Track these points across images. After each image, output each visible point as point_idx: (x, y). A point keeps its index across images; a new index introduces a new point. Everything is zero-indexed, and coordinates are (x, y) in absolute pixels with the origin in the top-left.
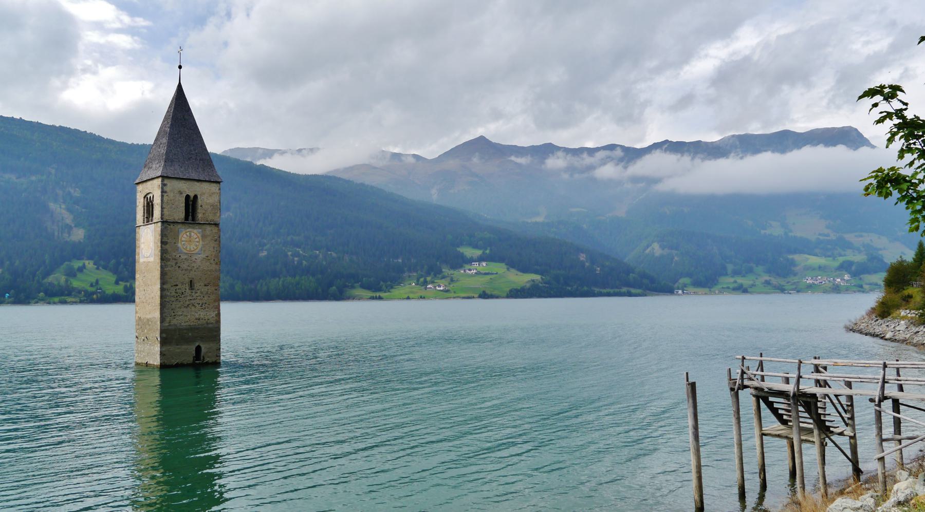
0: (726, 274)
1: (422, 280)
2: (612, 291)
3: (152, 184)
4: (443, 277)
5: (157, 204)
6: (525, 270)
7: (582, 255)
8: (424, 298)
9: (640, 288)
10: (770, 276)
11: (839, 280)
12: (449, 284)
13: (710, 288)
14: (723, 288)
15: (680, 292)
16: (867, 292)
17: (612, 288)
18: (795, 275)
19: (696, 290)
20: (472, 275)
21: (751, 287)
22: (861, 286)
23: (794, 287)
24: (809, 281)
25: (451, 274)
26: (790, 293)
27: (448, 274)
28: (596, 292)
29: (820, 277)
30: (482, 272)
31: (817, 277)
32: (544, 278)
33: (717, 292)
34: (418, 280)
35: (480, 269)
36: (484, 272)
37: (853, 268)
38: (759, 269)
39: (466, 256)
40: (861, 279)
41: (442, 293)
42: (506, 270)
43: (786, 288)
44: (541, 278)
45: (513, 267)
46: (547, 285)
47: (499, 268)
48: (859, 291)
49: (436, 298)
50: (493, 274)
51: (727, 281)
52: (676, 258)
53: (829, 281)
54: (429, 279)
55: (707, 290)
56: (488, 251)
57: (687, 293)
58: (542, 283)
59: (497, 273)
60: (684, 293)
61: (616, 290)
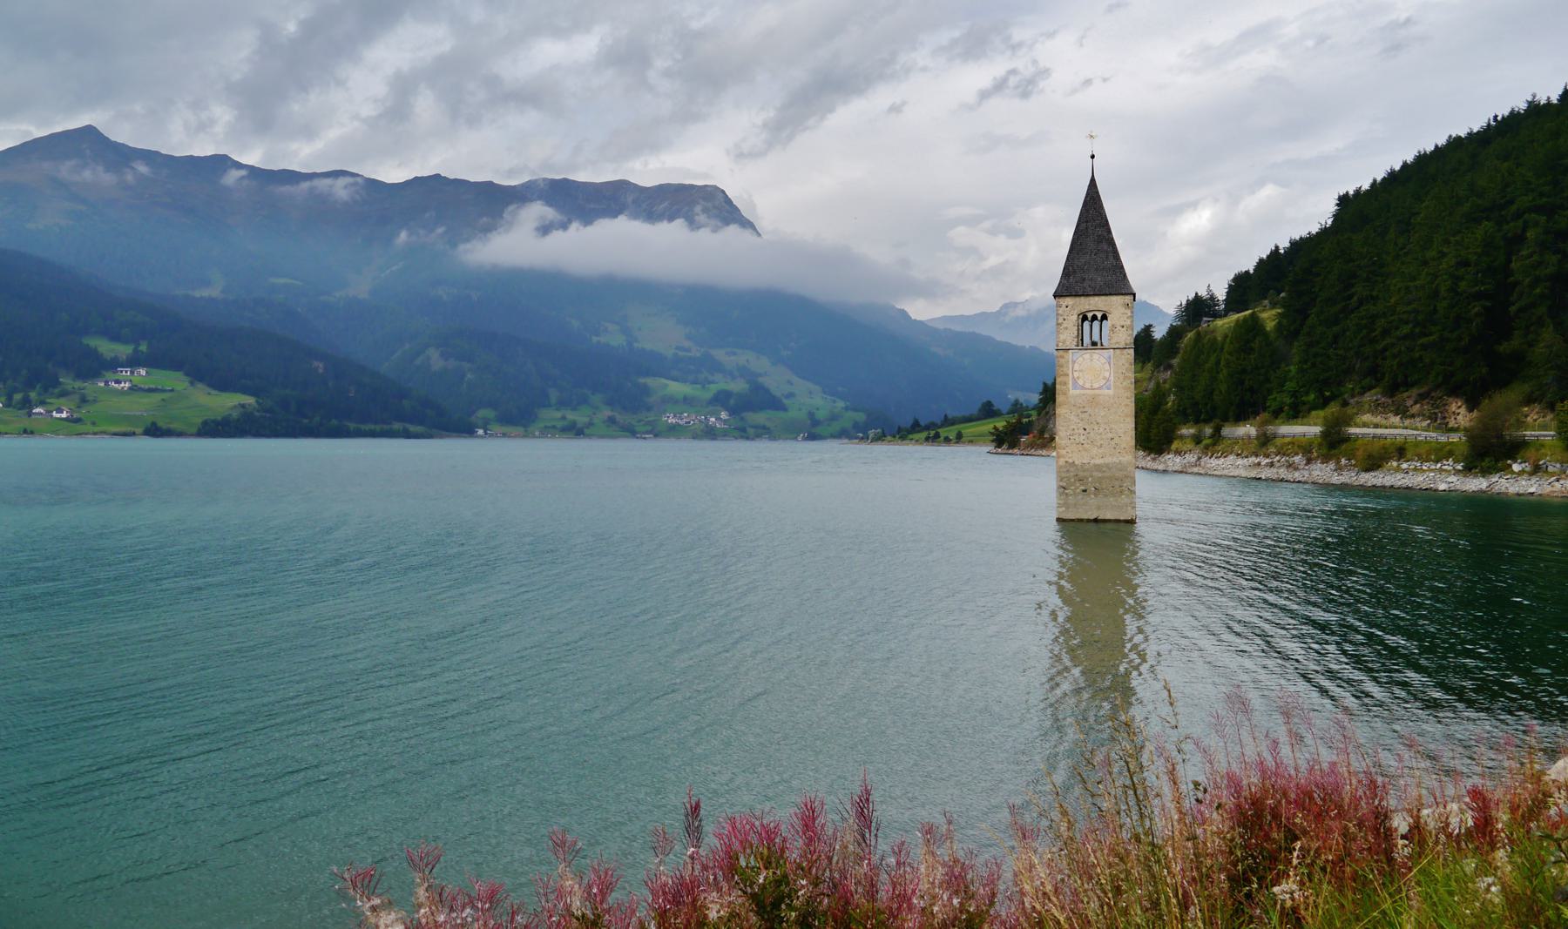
0: (550, 406)
1: (18, 397)
2: (378, 428)
3: (1106, 301)
4: (64, 394)
5: (1123, 327)
6: (223, 385)
7: (316, 364)
8: (32, 433)
9: (421, 423)
10: (612, 410)
11: (713, 419)
12: (79, 407)
13: (525, 426)
14: (546, 427)
15: (481, 432)
16: (753, 439)
17: (376, 423)
18: (649, 409)
19: (505, 429)
20: (122, 392)
21: (588, 427)
22: (743, 430)
23: (650, 428)
24: (671, 420)
25: (79, 389)
26: (645, 438)
27: (73, 388)
28: (352, 429)
29: (686, 415)
30: (143, 386)
31: (682, 414)
32: (261, 401)
33: (537, 433)
34: (10, 398)
35: (136, 379)
36: (147, 387)
37: (732, 402)
38: (596, 399)
39: (102, 354)
40: (742, 419)
41: (66, 423)
42: (186, 384)
43: (637, 429)
44: (257, 402)
45: (201, 380)
46: (268, 415)
47: (174, 381)
48: (742, 437)
49: (56, 432)
50: (163, 391)
51: (551, 415)
52: (469, 376)
53: (700, 421)
54: (33, 395)
55: (520, 430)
56: (143, 347)
57: (491, 435)
58: (258, 411)
59: (172, 390)
60: (486, 434)
61: (386, 427)
